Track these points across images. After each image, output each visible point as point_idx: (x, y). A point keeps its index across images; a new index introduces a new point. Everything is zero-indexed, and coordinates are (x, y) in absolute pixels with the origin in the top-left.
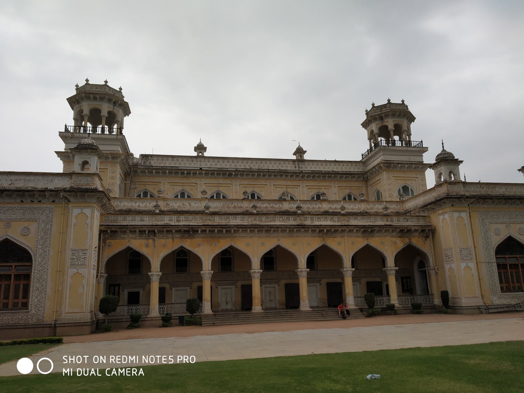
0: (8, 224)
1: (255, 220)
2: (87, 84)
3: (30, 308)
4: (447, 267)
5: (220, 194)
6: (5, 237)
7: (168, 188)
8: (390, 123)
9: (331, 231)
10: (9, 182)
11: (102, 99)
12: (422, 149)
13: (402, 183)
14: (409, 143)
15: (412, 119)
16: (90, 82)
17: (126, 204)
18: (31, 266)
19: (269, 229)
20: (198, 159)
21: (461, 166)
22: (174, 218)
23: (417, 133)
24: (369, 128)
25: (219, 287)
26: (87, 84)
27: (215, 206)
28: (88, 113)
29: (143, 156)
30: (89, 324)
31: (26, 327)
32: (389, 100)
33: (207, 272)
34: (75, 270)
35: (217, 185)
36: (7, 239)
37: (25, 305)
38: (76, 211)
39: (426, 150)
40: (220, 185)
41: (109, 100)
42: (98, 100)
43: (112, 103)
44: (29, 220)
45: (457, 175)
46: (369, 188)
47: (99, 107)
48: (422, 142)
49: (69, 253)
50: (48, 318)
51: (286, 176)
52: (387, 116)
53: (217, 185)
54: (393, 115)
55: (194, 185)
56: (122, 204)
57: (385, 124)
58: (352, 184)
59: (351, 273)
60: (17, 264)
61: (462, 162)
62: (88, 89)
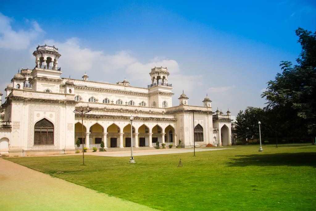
0: (45, 113)
8: (162, 76)
9: (146, 119)
13: (164, 100)
18: (53, 129)
28: (46, 60)
31: (54, 151)
34: (69, 131)
37: (53, 143)
44: (52, 111)
46: (150, 100)
50: (61, 148)
51: (120, 92)
52: (160, 73)
57: (159, 75)
58: (144, 98)
59: (151, 134)
60: (48, 128)
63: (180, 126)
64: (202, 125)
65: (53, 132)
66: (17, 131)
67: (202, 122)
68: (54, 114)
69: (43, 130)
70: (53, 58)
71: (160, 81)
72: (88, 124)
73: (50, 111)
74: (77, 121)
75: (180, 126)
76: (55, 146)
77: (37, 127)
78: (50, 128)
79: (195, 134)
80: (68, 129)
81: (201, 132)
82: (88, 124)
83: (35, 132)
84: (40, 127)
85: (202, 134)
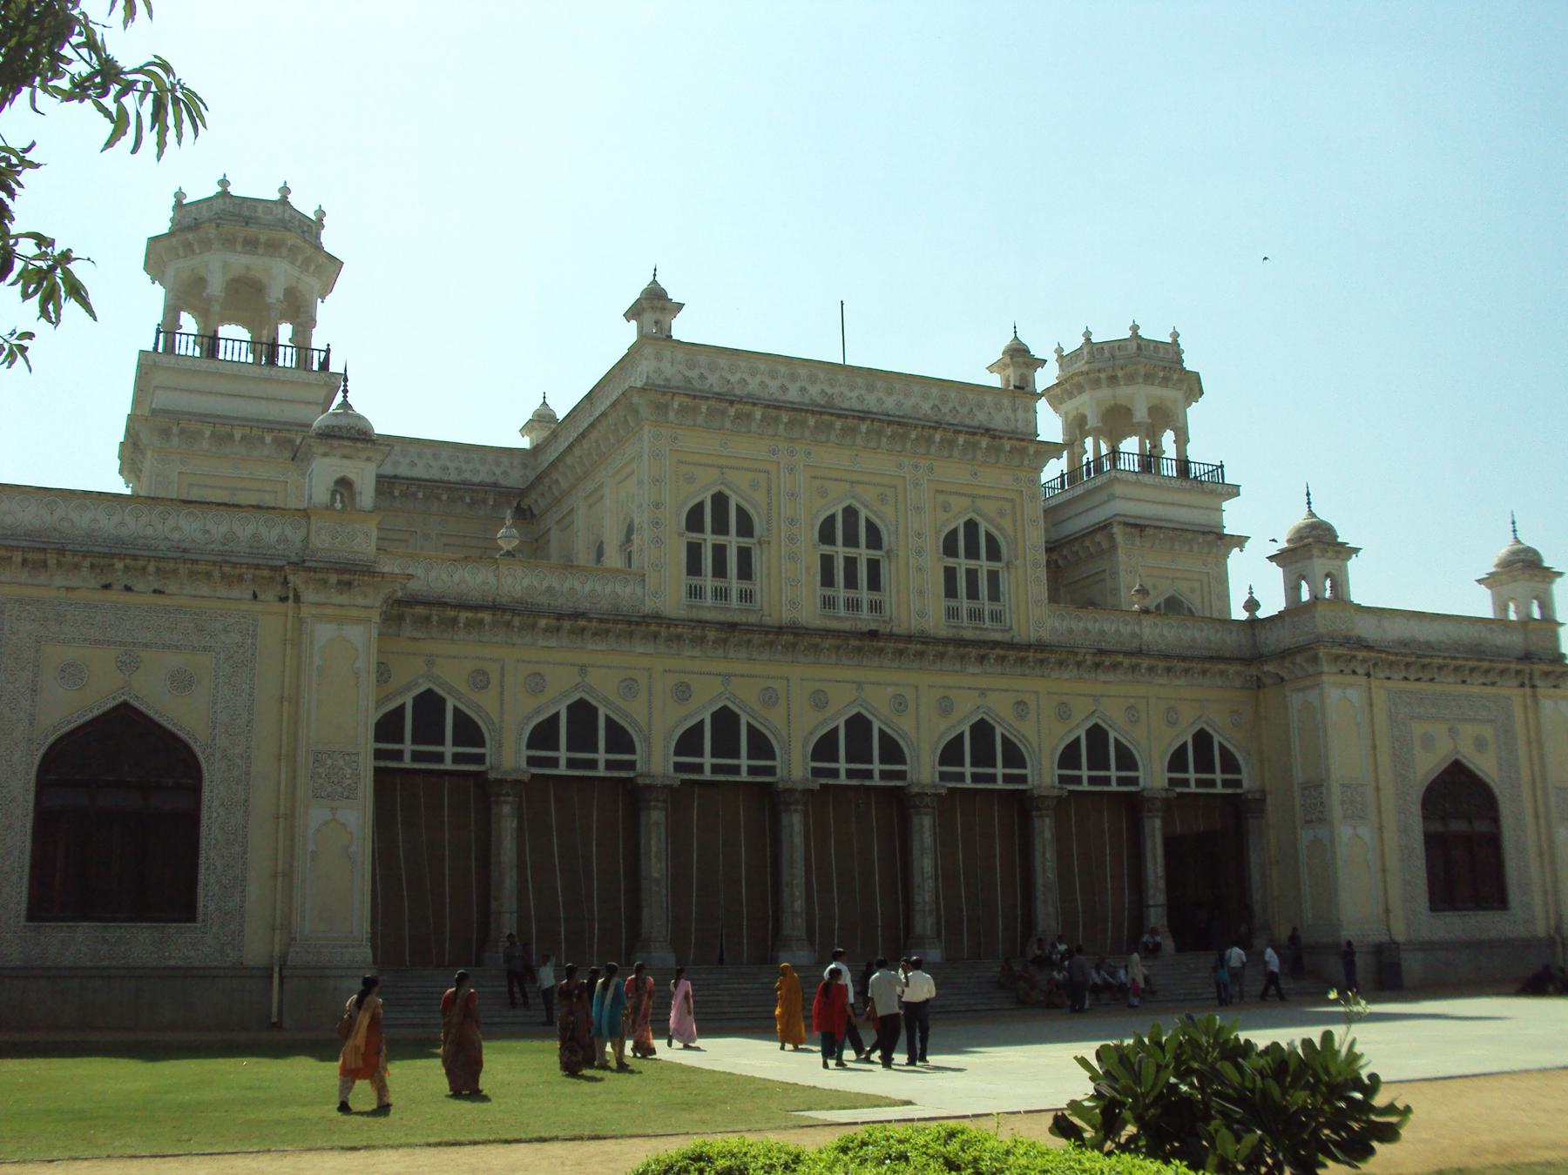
2: (224, 194)
3: (200, 917)
4: (1305, 836)
12: (1219, 488)
14: (1183, 465)
15: (1192, 386)
16: (234, 190)
18: (197, 790)
21: (1353, 564)
23: (1209, 435)
24: (1070, 405)
26: (224, 194)
32: (1135, 328)
36: (125, 704)
38: (324, 632)
39: (1234, 491)
45: (1340, 585)
48: (1222, 467)
54: (1149, 378)
61: (1356, 550)
63: (1299, 776)
64: (1486, 766)
67: (1480, 744)
70: (279, 274)
71: (1130, 445)
75: (1299, 776)
79: (1431, 840)
81: (1482, 826)
85: (1494, 841)
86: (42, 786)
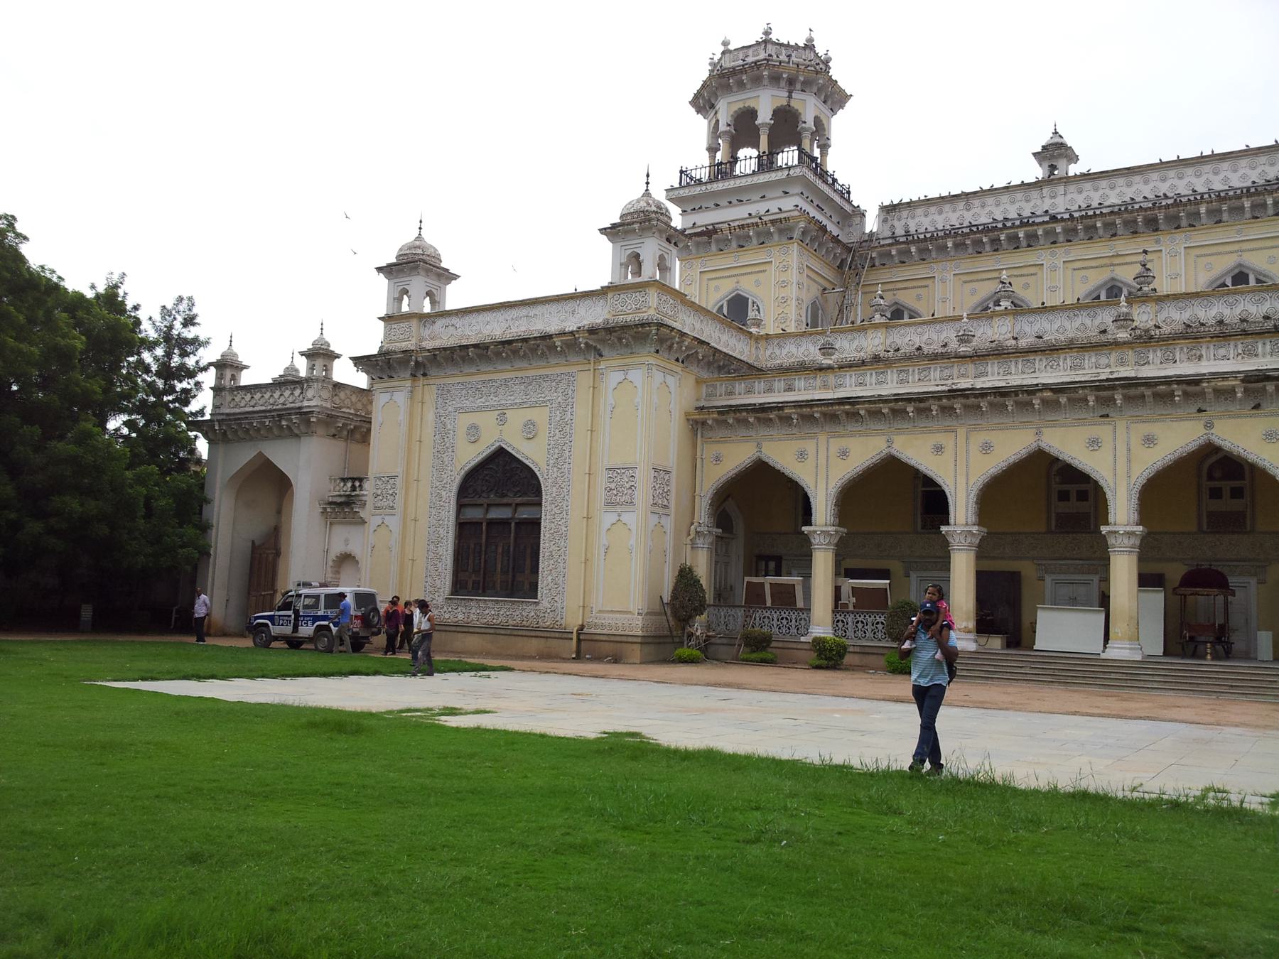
0: (502, 419)
1: (1122, 363)
5: (1121, 290)
6: (497, 444)
7: (949, 291)
10: (504, 325)
11: (757, 81)
17: (794, 350)
18: (540, 504)
19: (1160, 394)
20: (1046, 191)
22: (870, 377)
25: (1048, 579)
27: (998, 331)
29: (889, 210)
30: (639, 640)
33: (959, 530)
34: (612, 518)
35: (1107, 261)
37: (532, 591)
38: (615, 377)
40: (1117, 261)
41: (775, 79)
42: (766, 82)
43: (783, 83)
47: (751, 104)
49: (601, 480)
50: (572, 621)
53: (1107, 261)
55: (1032, 270)
56: (785, 352)
60: (519, 500)
62: (728, 63)
65: (535, 524)
66: (388, 520)
68: (540, 416)
69: (495, 514)
72: (823, 468)
73: (520, 406)
74: (734, 455)
76: (540, 607)
77: (466, 501)
78: (525, 499)
80: (609, 503)
82: (823, 468)
83: (464, 529)
84: (479, 502)
86: (460, 507)
